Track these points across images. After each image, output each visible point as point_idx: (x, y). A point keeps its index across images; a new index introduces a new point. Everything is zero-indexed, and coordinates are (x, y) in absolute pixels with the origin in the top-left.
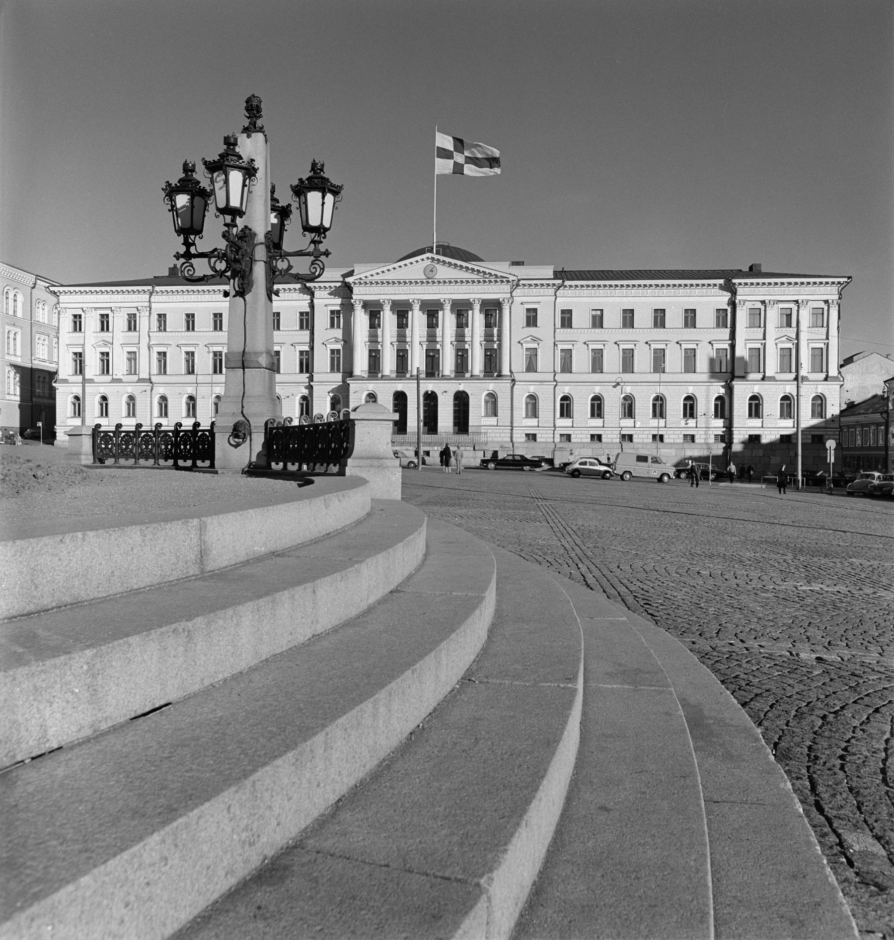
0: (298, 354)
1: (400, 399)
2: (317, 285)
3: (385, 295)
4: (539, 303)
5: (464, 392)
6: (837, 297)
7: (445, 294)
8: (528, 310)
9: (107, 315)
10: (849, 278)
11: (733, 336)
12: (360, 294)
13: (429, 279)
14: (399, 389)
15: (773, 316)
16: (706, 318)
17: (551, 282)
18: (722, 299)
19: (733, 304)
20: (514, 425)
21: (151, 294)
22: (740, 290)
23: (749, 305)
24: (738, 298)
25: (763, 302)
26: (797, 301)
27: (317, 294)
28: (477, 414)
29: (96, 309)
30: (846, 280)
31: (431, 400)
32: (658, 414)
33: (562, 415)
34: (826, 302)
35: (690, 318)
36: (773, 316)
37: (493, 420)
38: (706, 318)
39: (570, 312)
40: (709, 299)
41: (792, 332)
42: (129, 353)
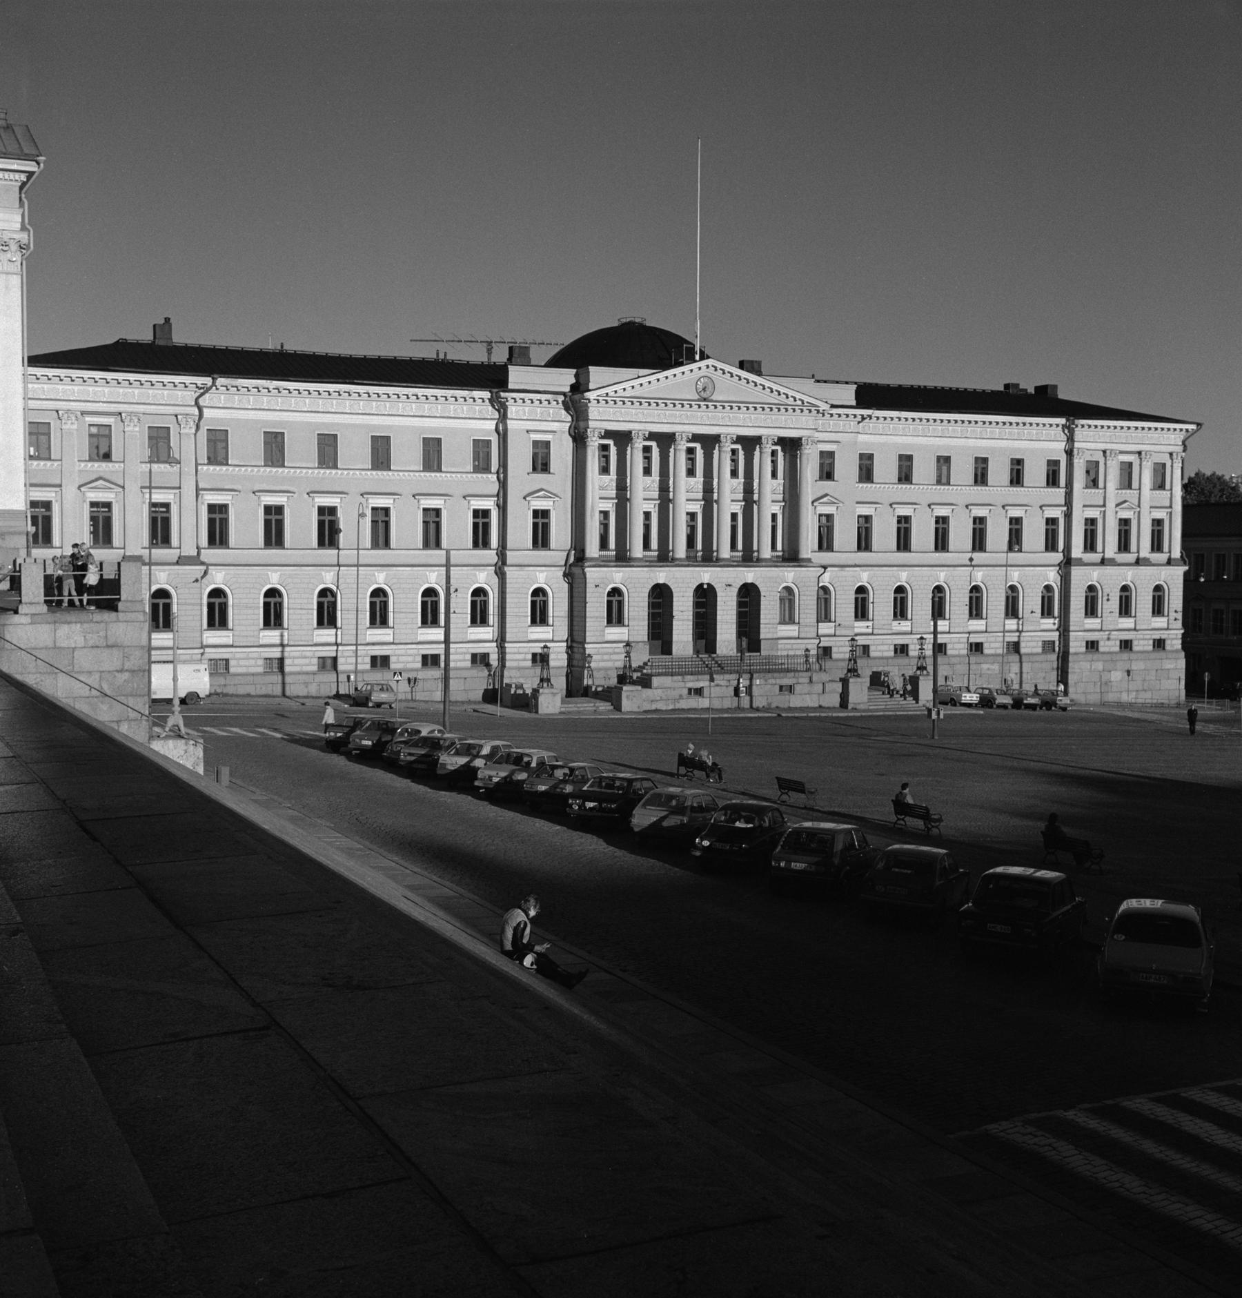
0: (261, 511)
1: (661, 597)
3: (641, 421)
6: (1181, 448)
7: (729, 425)
8: (536, 444)
10: (1198, 424)
11: (1068, 502)
13: (704, 398)
14: (750, 581)
16: (1035, 473)
19: (1069, 453)
20: (508, 637)
24: (1076, 445)
26: (1140, 453)
30: (1194, 427)
31: (705, 597)
33: (373, 622)
37: (791, 630)
39: (871, 457)
41: (1058, 494)
42: (93, 504)
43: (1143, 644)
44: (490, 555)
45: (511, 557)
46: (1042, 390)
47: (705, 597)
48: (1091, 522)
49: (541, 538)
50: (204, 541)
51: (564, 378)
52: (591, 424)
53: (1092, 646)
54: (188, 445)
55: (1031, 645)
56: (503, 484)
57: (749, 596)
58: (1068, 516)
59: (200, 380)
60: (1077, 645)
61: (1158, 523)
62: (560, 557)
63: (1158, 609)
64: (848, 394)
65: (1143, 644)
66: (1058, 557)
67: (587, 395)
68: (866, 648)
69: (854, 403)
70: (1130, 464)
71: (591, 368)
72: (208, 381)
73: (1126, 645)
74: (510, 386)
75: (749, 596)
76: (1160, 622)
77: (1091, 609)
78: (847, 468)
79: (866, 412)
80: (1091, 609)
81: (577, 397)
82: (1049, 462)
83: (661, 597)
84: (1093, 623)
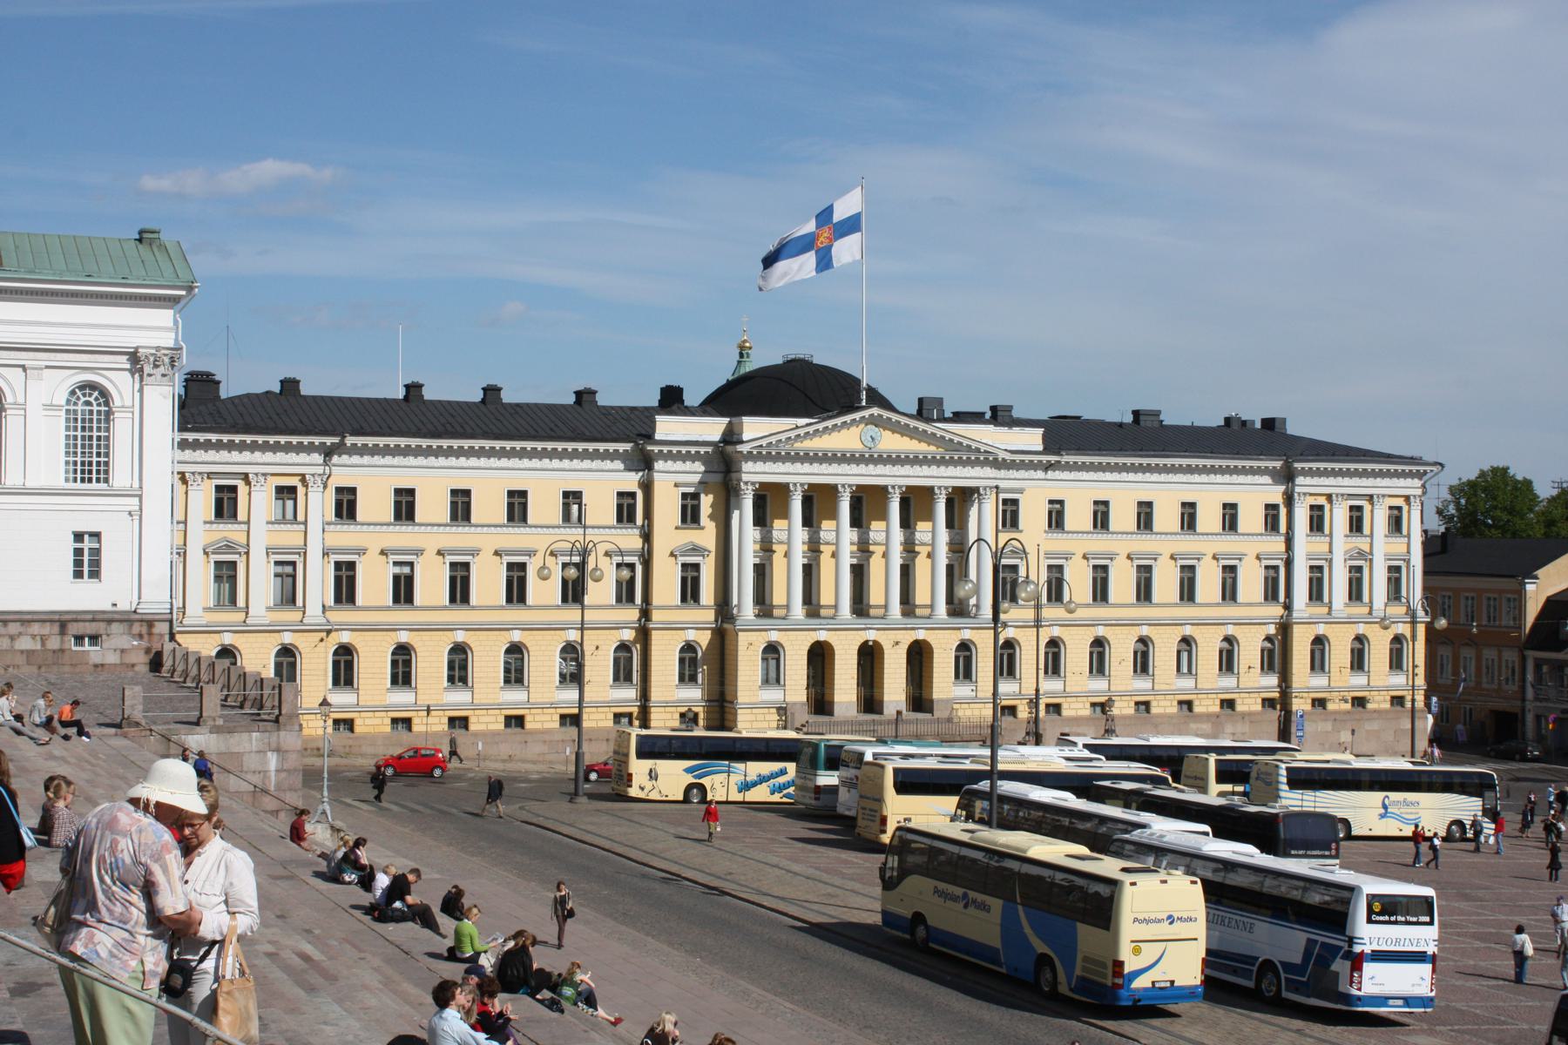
1: (820, 657)
2: (656, 449)
4: (1021, 491)
5: (925, 642)
9: (234, 489)
12: (753, 473)
15: (1339, 517)
16: (1251, 519)
17: (1036, 458)
18: (1275, 494)
19: (1289, 500)
21: (328, 452)
22: (1300, 480)
23: (1312, 501)
24: (1297, 489)
25: (1329, 497)
27: (659, 465)
28: (943, 682)
29: (210, 475)
31: (870, 656)
32: (1185, 670)
34: (1407, 498)
35: (1230, 516)
36: (1339, 517)
37: (965, 690)
38: (1251, 519)
40: (1254, 492)
43: (1379, 702)
44: (632, 614)
45: (656, 616)
46: (1269, 424)
47: (870, 656)
48: (1316, 569)
49: (690, 591)
50: (330, 601)
51: (711, 428)
52: (745, 477)
53: (1320, 703)
54: (318, 504)
55: (1249, 704)
56: (647, 537)
57: (919, 656)
58: (1289, 563)
59: (329, 441)
60: (1300, 705)
61: (1394, 570)
62: (710, 616)
63: (1396, 662)
64: (1032, 439)
65: (1379, 702)
66: (1277, 611)
67: (740, 448)
68: (1055, 708)
69: (1040, 448)
70: (1360, 509)
71: (746, 419)
72: (336, 440)
73: (1360, 702)
74: (658, 437)
75: (919, 656)
76: (1399, 680)
77: (1318, 662)
78: (1033, 515)
79: (1053, 458)
80: (1318, 662)
81: (729, 448)
82: (1267, 506)
83: (820, 657)
84: (1319, 681)
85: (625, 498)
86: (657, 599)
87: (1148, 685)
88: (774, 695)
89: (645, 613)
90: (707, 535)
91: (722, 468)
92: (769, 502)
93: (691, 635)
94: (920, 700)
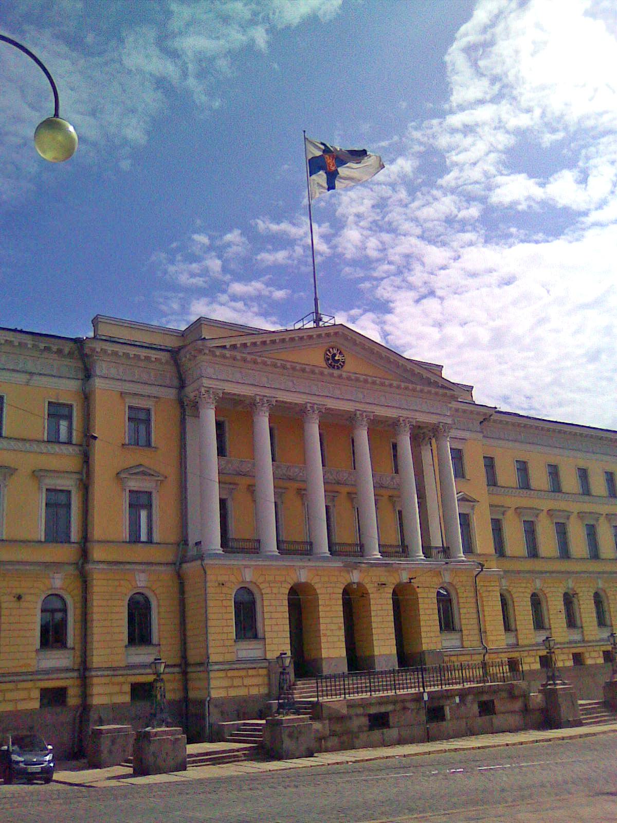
1: (300, 603)
31: (353, 604)
44: (65, 553)
45: (97, 553)
47: (353, 604)
83: (300, 603)
85: (58, 412)
86: (97, 533)
87: (578, 637)
88: (249, 650)
89: (85, 554)
90: (161, 459)
91: (176, 383)
92: (235, 415)
93: (142, 581)
94: (409, 658)
